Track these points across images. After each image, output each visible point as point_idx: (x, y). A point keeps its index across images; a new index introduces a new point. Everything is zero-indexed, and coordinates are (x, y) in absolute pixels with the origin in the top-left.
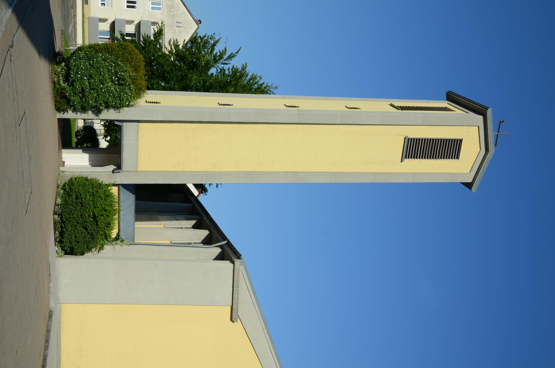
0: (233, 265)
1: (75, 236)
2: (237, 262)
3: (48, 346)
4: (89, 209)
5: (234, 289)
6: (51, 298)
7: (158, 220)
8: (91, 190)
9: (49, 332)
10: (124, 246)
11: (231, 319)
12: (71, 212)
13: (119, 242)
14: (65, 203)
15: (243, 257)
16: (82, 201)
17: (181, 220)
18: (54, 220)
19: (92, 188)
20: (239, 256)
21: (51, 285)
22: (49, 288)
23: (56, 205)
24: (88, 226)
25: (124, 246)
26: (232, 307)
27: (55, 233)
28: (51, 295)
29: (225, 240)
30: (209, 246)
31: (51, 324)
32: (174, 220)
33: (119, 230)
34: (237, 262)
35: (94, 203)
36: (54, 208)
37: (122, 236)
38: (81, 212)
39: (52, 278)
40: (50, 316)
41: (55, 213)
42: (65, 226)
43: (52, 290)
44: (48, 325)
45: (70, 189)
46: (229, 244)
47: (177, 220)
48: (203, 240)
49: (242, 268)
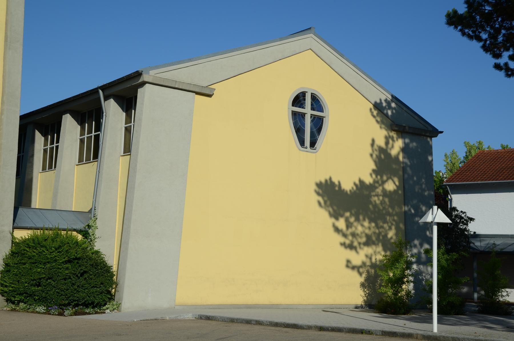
0: (147, 85)
1: (93, 287)
2: (145, 78)
4: (58, 268)
5: (176, 86)
6: (182, 317)
7: (31, 181)
8: (27, 266)
9: (234, 319)
10: (96, 225)
11: (210, 96)
12: (57, 292)
13: (90, 231)
14: (43, 300)
15: (139, 69)
16: (44, 277)
17: (33, 150)
18: (71, 315)
19: (25, 264)
20: (138, 74)
21: (168, 318)
22: (172, 321)
23: (48, 313)
24: (81, 270)
25: (96, 225)
26: (197, 93)
27: (89, 314)
28: (179, 318)
29: (98, 92)
30: (104, 114)
31: (221, 317)
32: (33, 159)
33: (75, 230)
34: (145, 78)
35: (48, 262)
36: (53, 315)
37: (81, 226)
38: (61, 279)
39: (159, 317)
40: (208, 318)
41: (61, 314)
42: (75, 301)
43: (173, 316)
44: (223, 321)
45: (20, 294)
46: (104, 88)
47: (33, 156)
48: (78, 124)
49: (152, 72)
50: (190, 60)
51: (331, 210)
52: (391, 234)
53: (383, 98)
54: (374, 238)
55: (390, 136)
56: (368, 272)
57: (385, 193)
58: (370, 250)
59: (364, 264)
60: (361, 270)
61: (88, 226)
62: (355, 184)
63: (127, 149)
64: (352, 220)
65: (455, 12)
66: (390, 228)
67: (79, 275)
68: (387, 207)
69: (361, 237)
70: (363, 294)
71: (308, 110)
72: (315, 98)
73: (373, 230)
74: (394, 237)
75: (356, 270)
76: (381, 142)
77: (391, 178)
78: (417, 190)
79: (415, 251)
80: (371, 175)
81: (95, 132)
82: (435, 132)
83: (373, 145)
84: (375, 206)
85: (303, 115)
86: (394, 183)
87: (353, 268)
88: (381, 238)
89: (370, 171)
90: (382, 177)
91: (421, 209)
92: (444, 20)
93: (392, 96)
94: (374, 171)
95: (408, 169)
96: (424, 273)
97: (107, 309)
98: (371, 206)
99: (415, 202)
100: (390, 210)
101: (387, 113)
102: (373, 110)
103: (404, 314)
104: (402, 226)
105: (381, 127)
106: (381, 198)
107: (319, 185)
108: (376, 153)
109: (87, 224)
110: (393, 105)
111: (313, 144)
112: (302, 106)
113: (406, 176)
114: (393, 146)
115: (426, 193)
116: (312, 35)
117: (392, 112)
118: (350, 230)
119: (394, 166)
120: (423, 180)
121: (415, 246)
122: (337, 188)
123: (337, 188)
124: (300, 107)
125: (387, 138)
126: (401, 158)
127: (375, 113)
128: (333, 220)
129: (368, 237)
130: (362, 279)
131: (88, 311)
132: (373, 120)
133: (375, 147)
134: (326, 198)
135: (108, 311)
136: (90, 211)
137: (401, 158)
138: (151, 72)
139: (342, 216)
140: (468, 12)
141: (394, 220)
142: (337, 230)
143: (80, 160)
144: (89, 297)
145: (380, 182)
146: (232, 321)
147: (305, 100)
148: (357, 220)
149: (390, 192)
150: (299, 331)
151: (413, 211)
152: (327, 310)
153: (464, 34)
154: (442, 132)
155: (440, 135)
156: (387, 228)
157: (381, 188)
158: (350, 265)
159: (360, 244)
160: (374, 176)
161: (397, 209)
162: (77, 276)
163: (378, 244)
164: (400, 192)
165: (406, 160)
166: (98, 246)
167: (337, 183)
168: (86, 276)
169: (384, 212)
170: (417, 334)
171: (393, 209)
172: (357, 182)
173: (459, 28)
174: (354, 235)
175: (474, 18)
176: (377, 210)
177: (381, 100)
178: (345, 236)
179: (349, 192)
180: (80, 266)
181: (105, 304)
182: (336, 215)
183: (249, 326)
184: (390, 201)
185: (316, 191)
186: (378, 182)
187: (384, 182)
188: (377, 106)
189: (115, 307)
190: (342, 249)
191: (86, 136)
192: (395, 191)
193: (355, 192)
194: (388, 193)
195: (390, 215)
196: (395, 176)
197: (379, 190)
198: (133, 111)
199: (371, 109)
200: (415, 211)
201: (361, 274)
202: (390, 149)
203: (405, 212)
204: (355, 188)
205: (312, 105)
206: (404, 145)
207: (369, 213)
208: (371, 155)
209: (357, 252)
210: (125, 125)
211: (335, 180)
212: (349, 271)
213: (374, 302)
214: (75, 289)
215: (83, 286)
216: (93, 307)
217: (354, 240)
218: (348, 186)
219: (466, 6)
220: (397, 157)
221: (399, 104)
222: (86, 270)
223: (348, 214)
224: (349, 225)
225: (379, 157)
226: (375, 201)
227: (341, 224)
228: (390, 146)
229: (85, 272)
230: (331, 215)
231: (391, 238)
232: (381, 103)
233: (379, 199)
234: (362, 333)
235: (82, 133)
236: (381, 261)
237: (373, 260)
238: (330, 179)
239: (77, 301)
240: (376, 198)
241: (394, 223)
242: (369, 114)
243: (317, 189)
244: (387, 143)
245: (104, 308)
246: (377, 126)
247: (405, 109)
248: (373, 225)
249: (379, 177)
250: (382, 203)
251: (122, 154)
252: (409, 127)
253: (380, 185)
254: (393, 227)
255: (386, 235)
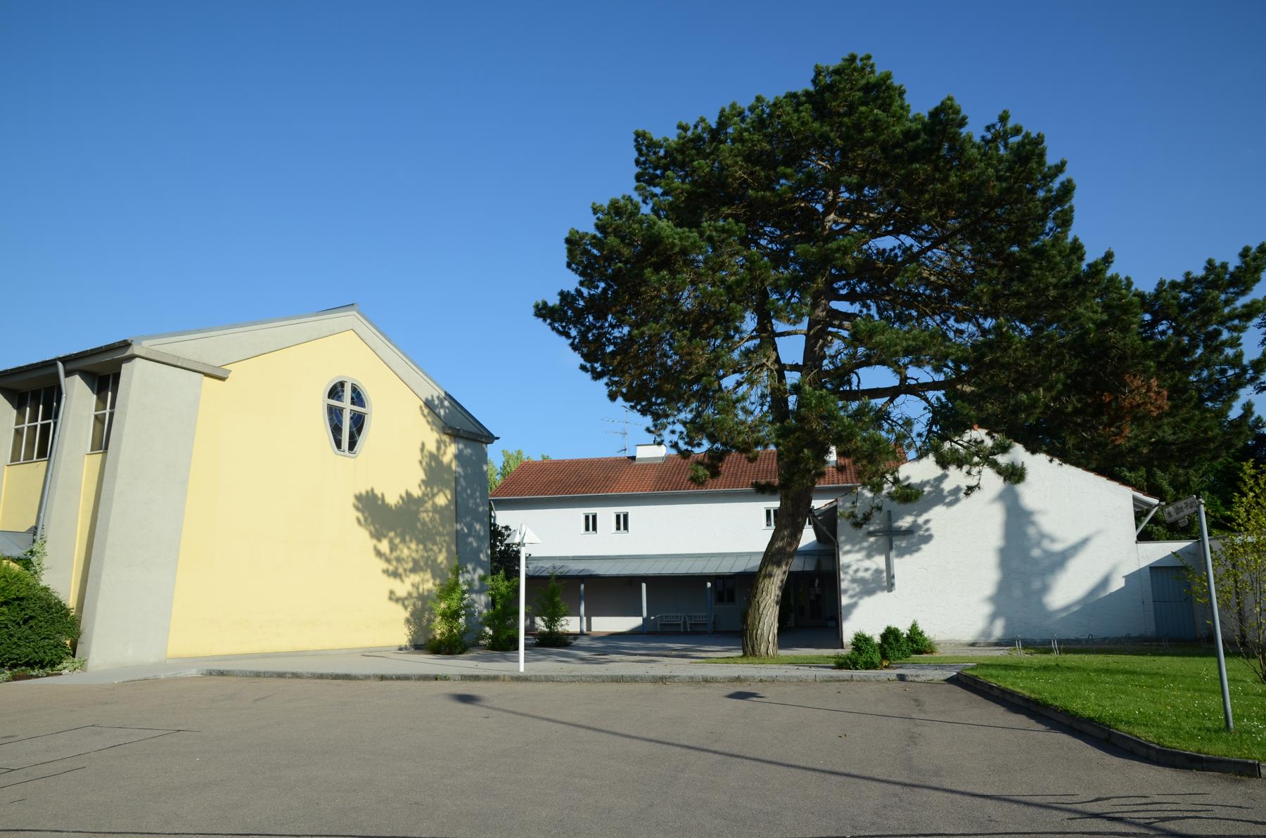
1: (44, 638)
2: (135, 350)
3: (293, 674)
5: (179, 364)
6: (182, 674)
9: (260, 673)
11: (223, 379)
13: (34, 559)
20: (126, 345)
21: (162, 677)
22: (168, 680)
27: (37, 677)
28: (178, 675)
29: (56, 365)
30: (64, 395)
31: (240, 671)
34: (135, 350)
39: (150, 675)
40: (222, 673)
42: (13, 659)
43: (170, 674)
46: (65, 360)
49: (145, 343)
50: (198, 331)
51: (372, 529)
52: (441, 558)
53: (435, 395)
54: (422, 563)
55: (442, 441)
56: (414, 605)
57: (436, 509)
58: (415, 578)
59: (410, 595)
60: (406, 603)
61: (31, 552)
62: (401, 497)
63: (102, 442)
64: (397, 541)
65: (545, 304)
66: (440, 551)
67: (21, 623)
68: (437, 525)
69: (407, 563)
70: (407, 632)
71: (346, 405)
72: (355, 390)
73: (421, 553)
74: (445, 562)
75: (400, 602)
76: (431, 447)
77: (442, 490)
78: (470, 505)
79: (468, 576)
80: (420, 486)
81: (42, 420)
82: (491, 438)
83: (422, 449)
84: (424, 524)
85: (341, 410)
86: (446, 497)
87: (397, 600)
88: (430, 562)
89: (419, 481)
90: (432, 489)
91: (475, 528)
92: (532, 311)
93: (446, 393)
94: (423, 481)
95: (462, 480)
96: (476, 602)
97: (64, 668)
98: (419, 525)
99: (468, 519)
100: (441, 529)
101: (439, 413)
102: (424, 408)
103: (460, 653)
104: (453, 548)
105: (432, 429)
106: (431, 514)
107: (359, 498)
108: (426, 460)
109: (29, 549)
110: (446, 403)
111: (352, 445)
112: (339, 398)
113: (459, 488)
114: (445, 453)
115: (481, 509)
116: (354, 313)
117: (445, 412)
118: (395, 554)
119: (446, 476)
120: (478, 494)
121: (468, 572)
122: (380, 502)
123: (380, 502)
124: (337, 400)
125: (439, 442)
126: (454, 466)
127: (426, 411)
128: (375, 542)
129: (415, 562)
130: (407, 614)
131: (34, 674)
132: (423, 420)
133: (425, 452)
134: (366, 515)
135: (67, 671)
136: (34, 530)
137: (454, 466)
138: (143, 342)
139: (385, 536)
140: (561, 305)
141: (445, 541)
142: (379, 554)
143: (15, 458)
144: (37, 653)
145: (430, 495)
146: (258, 675)
147: (343, 391)
148: (403, 541)
149: (441, 507)
150: (353, 683)
151: (466, 531)
152: (368, 653)
153: (553, 328)
154: (498, 438)
155: (496, 441)
156: (437, 551)
157: (430, 502)
158: (393, 597)
159: (405, 570)
160: (423, 488)
161: (448, 528)
162: (18, 624)
163: (426, 571)
164: (452, 507)
165: (459, 470)
166: (46, 580)
167: (380, 495)
168: (32, 623)
169: (434, 531)
170: (504, 676)
171: (444, 527)
172: (404, 495)
173: (548, 321)
174: (399, 560)
175: (566, 312)
176: (425, 528)
177: (432, 397)
178: (388, 561)
179: (394, 507)
180: (23, 609)
181: (60, 662)
182: (378, 536)
183: (283, 680)
184: (440, 518)
185: (354, 505)
186: (427, 495)
187: (434, 495)
188: (428, 404)
189: (78, 664)
190: (385, 577)
191: (26, 424)
192: (446, 506)
193: (401, 507)
194: (439, 508)
195: (441, 534)
196: (447, 488)
197: (429, 505)
198: (110, 393)
199: (421, 407)
200: (468, 530)
201: (406, 607)
202: (442, 456)
203: (457, 531)
204: (401, 502)
205: (352, 398)
206: (457, 451)
207: (417, 533)
208: (421, 462)
209: (402, 581)
210: (96, 411)
211: (378, 492)
212: (392, 605)
213: (421, 641)
214: (15, 643)
215: (26, 638)
216: (42, 667)
217: (399, 566)
218: (392, 499)
219: (559, 297)
220: (449, 466)
221: (453, 403)
222: (33, 614)
223: (392, 534)
224: (393, 548)
225: (429, 465)
226: (424, 519)
227: (384, 546)
228: (442, 452)
229: (31, 618)
230: (373, 536)
231: (442, 563)
232: (433, 400)
233: (428, 516)
234: (436, 679)
235: (20, 419)
236: (429, 591)
237: (421, 590)
238: (372, 490)
239: (16, 659)
240: (424, 515)
241: (445, 545)
242: (419, 412)
243: (356, 503)
244: (439, 448)
245: (59, 667)
246: (428, 427)
247: (459, 409)
248: (421, 547)
249: (429, 489)
250: (432, 520)
251: (89, 452)
252: (464, 431)
253: (430, 499)
254: (444, 550)
255: (435, 560)
